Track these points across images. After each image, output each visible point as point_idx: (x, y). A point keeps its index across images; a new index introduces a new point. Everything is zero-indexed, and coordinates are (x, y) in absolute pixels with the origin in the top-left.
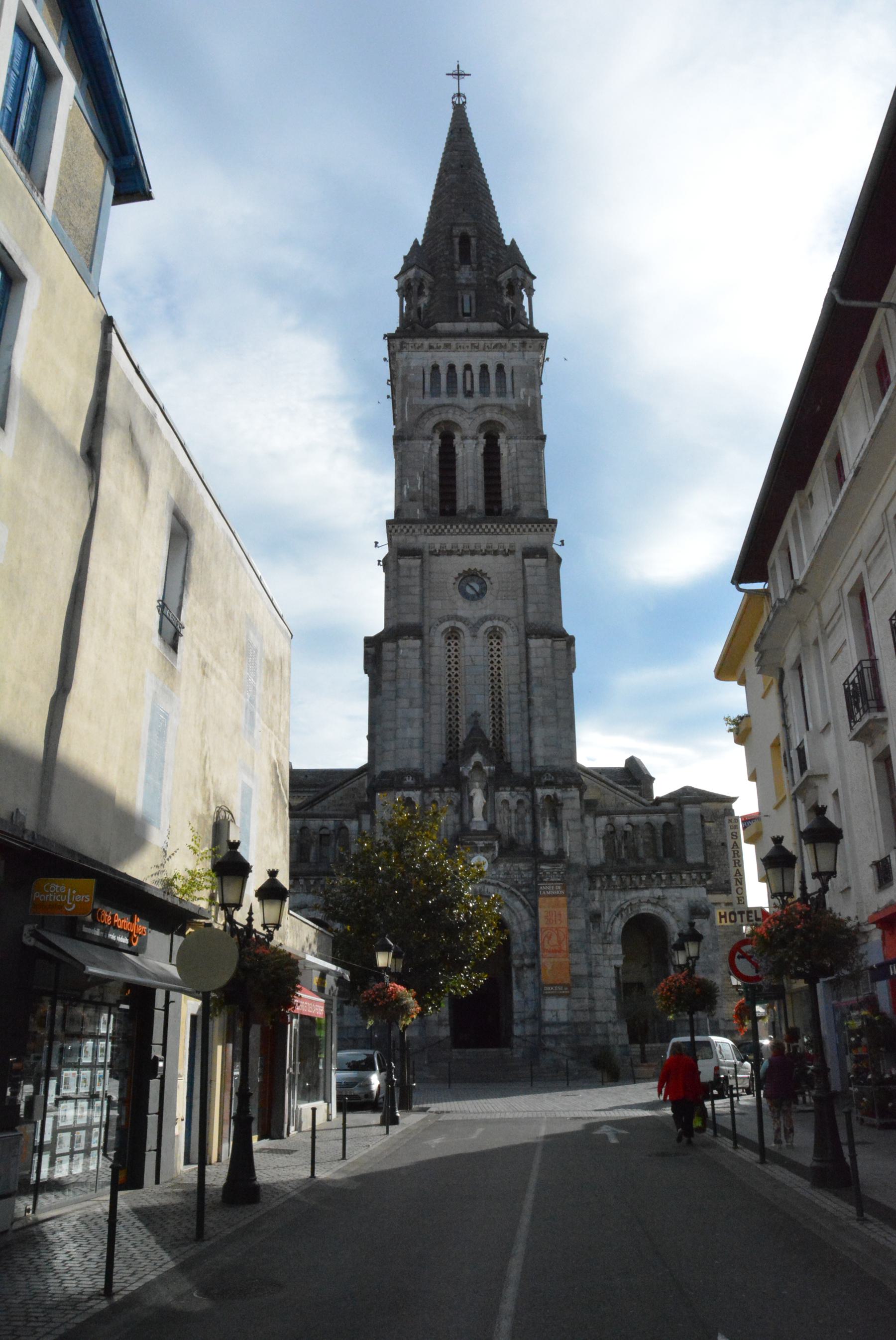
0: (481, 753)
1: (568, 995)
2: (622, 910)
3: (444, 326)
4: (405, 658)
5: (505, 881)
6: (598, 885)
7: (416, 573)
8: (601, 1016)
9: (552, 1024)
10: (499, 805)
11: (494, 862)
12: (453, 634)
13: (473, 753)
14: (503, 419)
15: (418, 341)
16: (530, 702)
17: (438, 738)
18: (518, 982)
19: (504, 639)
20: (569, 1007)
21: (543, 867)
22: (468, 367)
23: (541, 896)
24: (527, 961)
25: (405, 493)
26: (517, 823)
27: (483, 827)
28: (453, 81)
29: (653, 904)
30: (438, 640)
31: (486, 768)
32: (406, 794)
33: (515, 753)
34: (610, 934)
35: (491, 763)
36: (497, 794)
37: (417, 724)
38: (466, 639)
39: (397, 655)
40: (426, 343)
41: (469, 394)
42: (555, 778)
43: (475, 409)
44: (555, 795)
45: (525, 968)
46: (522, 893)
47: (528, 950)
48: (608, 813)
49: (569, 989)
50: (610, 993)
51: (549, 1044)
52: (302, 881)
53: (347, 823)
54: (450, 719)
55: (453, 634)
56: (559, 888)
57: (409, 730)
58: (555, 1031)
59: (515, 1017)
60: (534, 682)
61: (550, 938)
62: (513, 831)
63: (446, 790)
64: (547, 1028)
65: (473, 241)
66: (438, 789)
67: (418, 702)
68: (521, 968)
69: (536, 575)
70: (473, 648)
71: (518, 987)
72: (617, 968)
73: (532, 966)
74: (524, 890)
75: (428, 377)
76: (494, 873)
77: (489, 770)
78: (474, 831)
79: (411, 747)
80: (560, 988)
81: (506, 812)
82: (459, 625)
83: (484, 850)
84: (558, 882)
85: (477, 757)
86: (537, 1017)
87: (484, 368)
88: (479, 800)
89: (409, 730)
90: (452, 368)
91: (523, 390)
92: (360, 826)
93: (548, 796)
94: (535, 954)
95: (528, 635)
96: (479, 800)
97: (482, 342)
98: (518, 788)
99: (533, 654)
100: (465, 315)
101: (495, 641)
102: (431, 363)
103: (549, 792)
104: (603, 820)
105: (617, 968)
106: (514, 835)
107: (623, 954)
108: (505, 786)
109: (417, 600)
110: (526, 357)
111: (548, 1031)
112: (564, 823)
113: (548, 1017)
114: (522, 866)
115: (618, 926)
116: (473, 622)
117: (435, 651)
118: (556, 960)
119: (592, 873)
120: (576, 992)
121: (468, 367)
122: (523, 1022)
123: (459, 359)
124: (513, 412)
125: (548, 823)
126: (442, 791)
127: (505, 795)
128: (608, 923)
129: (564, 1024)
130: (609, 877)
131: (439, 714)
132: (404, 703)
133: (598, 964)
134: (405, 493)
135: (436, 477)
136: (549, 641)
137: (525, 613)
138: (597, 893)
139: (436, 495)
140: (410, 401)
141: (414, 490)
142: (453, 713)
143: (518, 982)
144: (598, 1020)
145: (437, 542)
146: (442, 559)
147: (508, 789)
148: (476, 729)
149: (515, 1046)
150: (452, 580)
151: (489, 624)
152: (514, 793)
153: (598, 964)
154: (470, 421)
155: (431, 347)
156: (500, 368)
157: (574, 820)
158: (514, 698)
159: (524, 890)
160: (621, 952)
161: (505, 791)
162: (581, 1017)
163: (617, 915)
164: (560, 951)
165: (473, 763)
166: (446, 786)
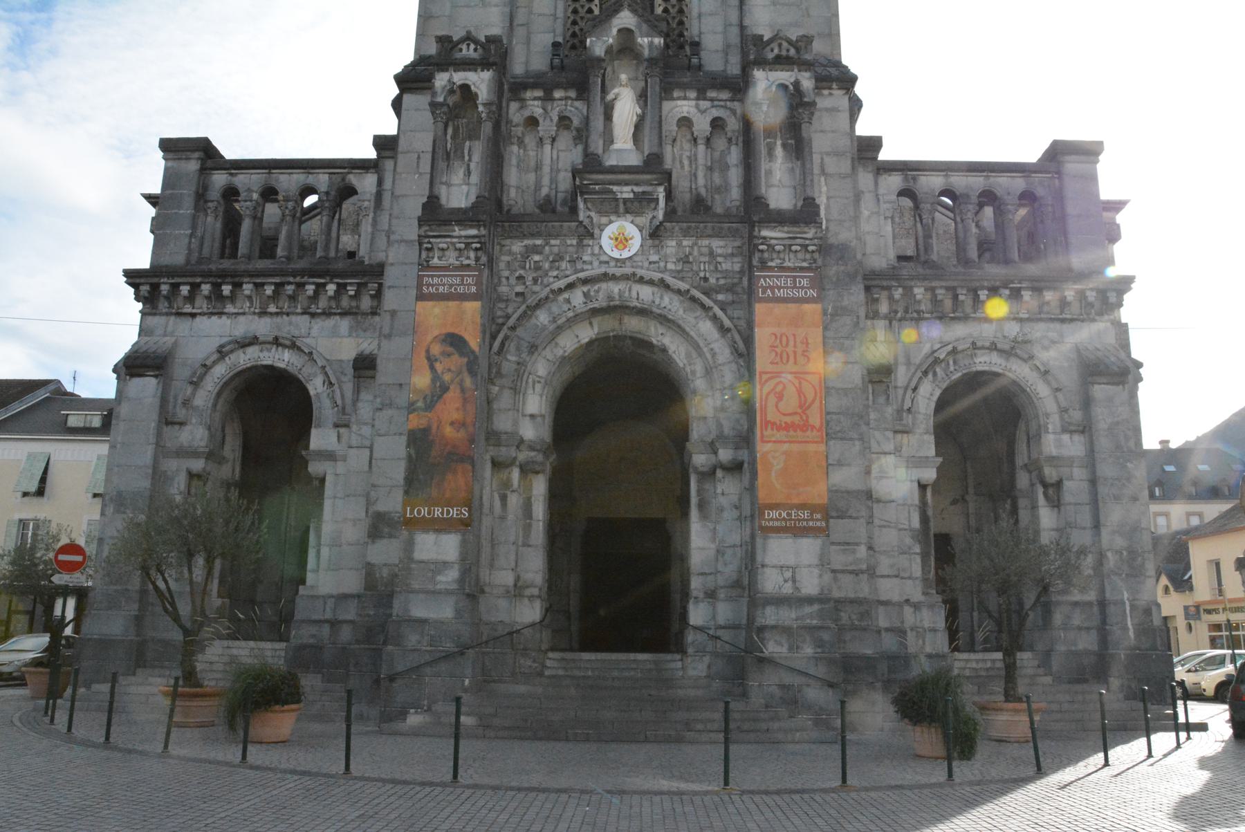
0: (634, 11)
1: (823, 532)
2: (937, 361)
5: (678, 275)
6: (884, 308)
8: (889, 589)
9: (780, 601)
10: (670, 127)
11: (655, 234)
13: (617, 11)
18: (702, 506)
20: (823, 562)
21: (765, 233)
23: (761, 300)
24: (725, 455)
27: (634, 160)
29: (1001, 352)
31: (643, 41)
32: (459, 77)
34: (909, 410)
35: (654, 28)
36: (667, 105)
42: (798, 50)
44: (797, 84)
45: (719, 473)
46: (716, 302)
47: (726, 431)
49: (827, 518)
50: (908, 541)
51: (774, 647)
52: (248, 288)
53: (353, 179)
56: (805, 282)
58: (787, 616)
59: (695, 584)
61: (780, 397)
62: (701, 181)
63: (558, 94)
64: (769, 610)
66: (539, 93)
68: (709, 475)
73: (735, 468)
74: (720, 297)
76: (654, 258)
77: (651, 44)
78: (612, 166)
80: (805, 514)
81: (687, 146)
83: (633, 207)
84: (802, 269)
85: (625, 19)
86: (745, 583)
88: (626, 108)
92: (380, 182)
93: (784, 87)
94: (745, 440)
96: (626, 108)
98: (712, 94)
104: (894, 182)
106: (703, 191)
107: (937, 455)
108: (684, 87)
112: (816, 158)
113: (771, 582)
114: (717, 244)
115: (928, 395)
118: (795, 447)
119: (873, 282)
120: (839, 528)
122: (711, 595)
125: (779, 151)
126: (548, 98)
127: (683, 106)
128: (906, 388)
129: (810, 600)
130: (908, 291)
144: (883, 598)
147: (693, 94)
149: (690, 650)
152: (704, 104)
157: (837, 154)
159: (720, 297)
160: (932, 452)
161: (685, 98)
162: (847, 588)
163: (925, 373)
164: (805, 427)
165: (615, 31)
166: (558, 86)
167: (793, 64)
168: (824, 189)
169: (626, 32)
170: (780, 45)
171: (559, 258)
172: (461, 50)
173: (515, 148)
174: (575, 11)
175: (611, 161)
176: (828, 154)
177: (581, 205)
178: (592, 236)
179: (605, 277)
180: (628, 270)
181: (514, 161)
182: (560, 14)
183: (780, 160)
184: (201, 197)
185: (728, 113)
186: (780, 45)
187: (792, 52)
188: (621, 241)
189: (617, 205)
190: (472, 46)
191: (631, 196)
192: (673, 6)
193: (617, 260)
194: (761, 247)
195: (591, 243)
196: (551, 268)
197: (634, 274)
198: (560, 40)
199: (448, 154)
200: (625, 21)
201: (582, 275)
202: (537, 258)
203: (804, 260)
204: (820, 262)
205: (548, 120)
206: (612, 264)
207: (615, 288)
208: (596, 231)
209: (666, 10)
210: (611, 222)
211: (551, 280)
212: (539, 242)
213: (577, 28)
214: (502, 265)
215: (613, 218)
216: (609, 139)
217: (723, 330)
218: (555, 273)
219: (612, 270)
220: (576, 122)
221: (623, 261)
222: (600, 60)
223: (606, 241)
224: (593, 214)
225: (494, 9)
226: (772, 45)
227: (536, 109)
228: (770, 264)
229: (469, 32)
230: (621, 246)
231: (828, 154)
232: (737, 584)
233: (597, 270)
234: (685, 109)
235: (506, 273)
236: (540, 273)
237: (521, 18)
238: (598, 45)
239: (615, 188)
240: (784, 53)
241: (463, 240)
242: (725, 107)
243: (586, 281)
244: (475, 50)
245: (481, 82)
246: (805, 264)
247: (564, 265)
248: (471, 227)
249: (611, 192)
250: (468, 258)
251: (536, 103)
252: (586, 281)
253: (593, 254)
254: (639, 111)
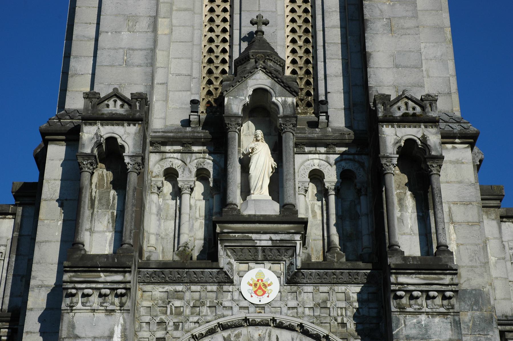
11: (292, 279)
31: (278, 100)
32: (106, 131)
42: (423, 108)
57: (125, 34)
63: (195, 149)
76: (292, 303)
77: (284, 103)
79: (127, 64)
85: (260, 80)
89: (125, 34)
93: (410, 142)
167: (420, 122)
168: (454, 237)
170: (406, 104)
171: (198, 304)
172: (108, 106)
173: (154, 197)
174: (210, 72)
175: (249, 211)
176: (455, 203)
177: (221, 252)
178: (231, 282)
179: (248, 322)
180: (267, 315)
181: (154, 210)
182: (195, 74)
183: (410, 210)
185: (357, 165)
186: (406, 104)
187: (418, 110)
188: (260, 287)
189: (257, 251)
190: (119, 103)
191: (270, 243)
192: (301, 68)
193: (257, 306)
194: (399, 293)
195: (230, 288)
196: (192, 314)
197: (274, 320)
198: (197, 98)
199: (92, 202)
200: (260, 82)
201: (222, 321)
202: (177, 303)
203: (443, 306)
204: (457, 306)
205: (187, 172)
206: (252, 309)
208: (236, 278)
209: (294, 72)
210: (249, 269)
211: (192, 325)
212: (179, 288)
213: (212, 88)
214: (143, 311)
215: (252, 265)
216: (246, 190)
218: (195, 319)
219: (253, 315)
221: (262, 307)
222: (236, 117)
224: (232, 261)
225: (136, 69)
226: (399, 104)
227: (174, 161)
228: (409, 309)
229: (115, 89)
230: (260, 292)
231: (455, 203)
233: (238, 315)
234: (316, 162)
235: (147, 319)
236: (181, 318)
237: (159, 78)
238: (235, 104)
239: (254, 236)
240: (411, 111)
241: (108, 285)
242: (353, 160)
243: (224, 327)
244: (122, 106)
245: (127, 135)
246: (442, 310)
247: (205, 310)
248: (116, 272)
249: (251, 240)
250: (113, 304)
251: (175, 155)
252: (224, 327)
253: (233, 300)
254: (274, 164)
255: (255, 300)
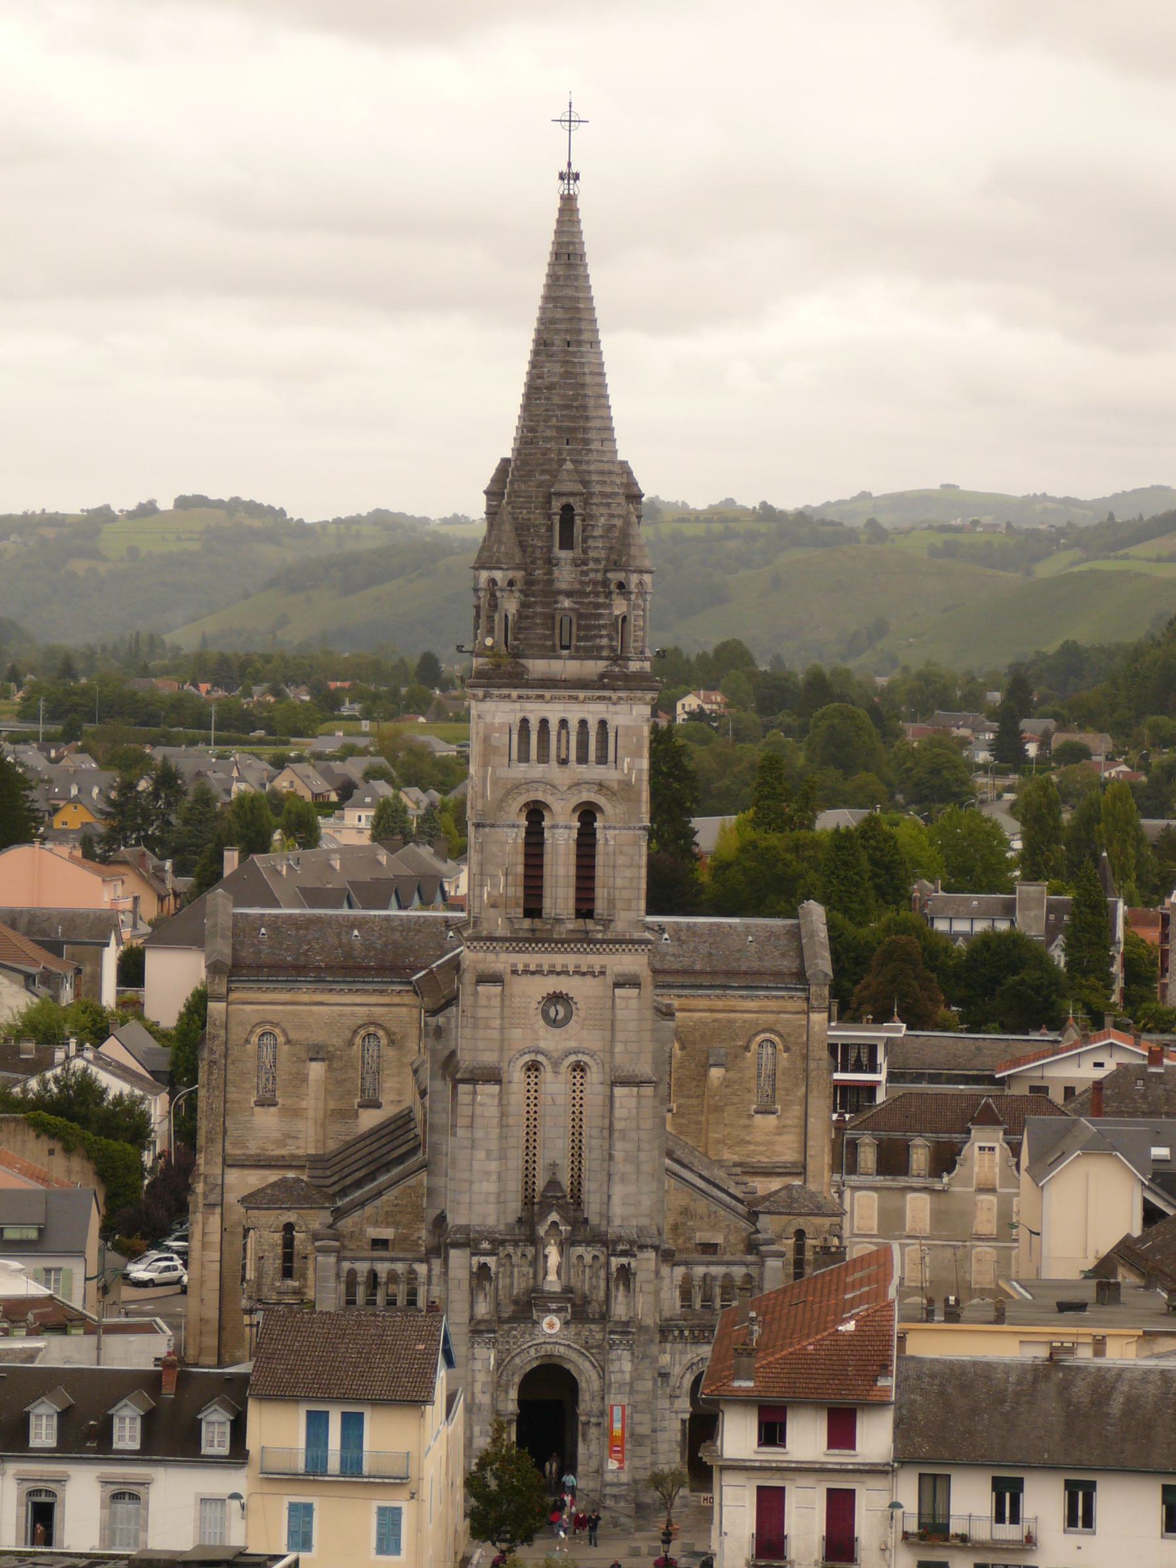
0: (558, 1213)
3: (537, 666)
4: (481, 1105)
7: (496, 1002)
9: (612, 1485)
11: (566, 1323)
12: (533, 1067)
14: (601, 800)
15: (505, 691)
16: (611, 1157)
17: (515, 1185)
19: (588, 1074)
22: (563, 723)
25: (485, 896)
26: (591, 1278)
27: (557, 1288)
28: (561, 131)
30: (517, 1075)
31: (562, 1228)
32: (483, 1259)
33: (592, 1208)
37: (494, 1177)
38: (547, 1074)
39: (474, 1099)
40: (514, 693)
41: (564, 762)
43: (570, 788)
44: (629, 1264)
48: (686, 1263)
50: (674, 1446)
51: (609, 1502)
54: (527, 1162)
55: (533, 1067)
60: (616, 1135)
65: (578, 521)
67: (495, 1154)
69: (626, 1008)
70: (555, 1085)
71: (584, 1440)
72: (683, 1421)
75: (515, 737)
79: (487, 1202)
82: (540, 1058)
85: (554, 1217)
87: (583, 723)
88: (553, 1257)
89: (485, 1184)
90: (544, 723)
91: (627, 760)
92: (430, 1270)
93: (623, 1265)
95: (613, 1084)
97: (581, 694)
99: (617, 1104)
100: (563, 647)
101: (578, 1074)
102: (520, 716)
103: (624, 1260)
104: (680, 1271)
105: (683, 1421)
109: (496, 1034)
110: (634, 713)
111: (608, 1490)
116: (555, 1055)
117: (514, 1087)
121: (563, 723)
123: (554, 712)
124: (614, 794)
127: (579, 1250)
129: (623, 1484)
131: (516, 1160)
132: (480, 1155)
133: (663, 1419)
134: (485, 896)
135: (520, 869)
136: (635, 1089)
137: (612, 1053)
138: (668, 1346)
139: (520, 892)
140: (493, 772)
141: (495, 893)
142: (531, 1154)
143: (584, 1435)
145: (521, 960)
146: (525, 980)
148: (553, 1184)
150: (534, 1005)
151: (572, 1058)
152: (589, 1249)
153: (663, 1419)
154: (562, 803)
155: (520, 697)
156: (603, 724)
157: (648, 1282)
158: (595, 1142)
169: (554, 1224)
184: (338, 1276)
207: (549, 1347)
217: (595, 1367)
220: (529, 1257)
223: (545, 1325)
232: (597, 1472)
233: (542, 1340)
255: (549, 1331)
